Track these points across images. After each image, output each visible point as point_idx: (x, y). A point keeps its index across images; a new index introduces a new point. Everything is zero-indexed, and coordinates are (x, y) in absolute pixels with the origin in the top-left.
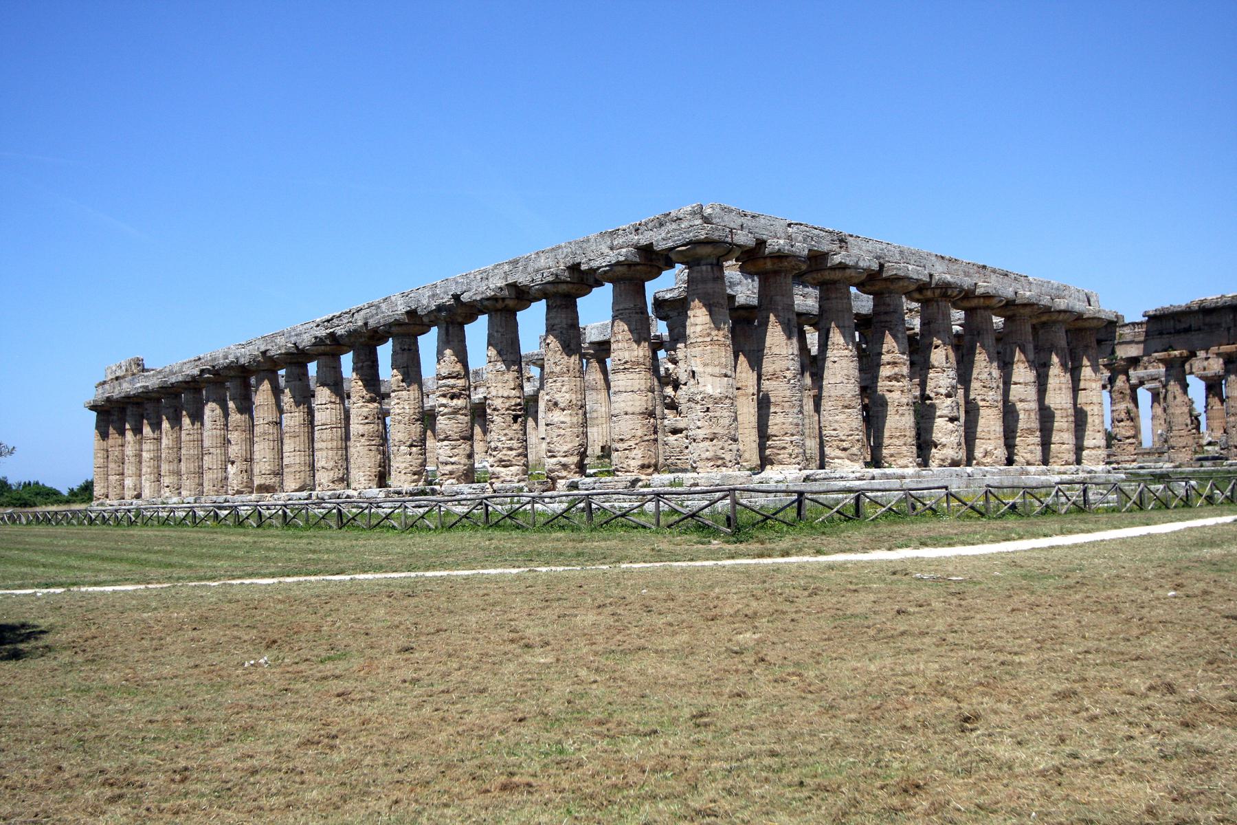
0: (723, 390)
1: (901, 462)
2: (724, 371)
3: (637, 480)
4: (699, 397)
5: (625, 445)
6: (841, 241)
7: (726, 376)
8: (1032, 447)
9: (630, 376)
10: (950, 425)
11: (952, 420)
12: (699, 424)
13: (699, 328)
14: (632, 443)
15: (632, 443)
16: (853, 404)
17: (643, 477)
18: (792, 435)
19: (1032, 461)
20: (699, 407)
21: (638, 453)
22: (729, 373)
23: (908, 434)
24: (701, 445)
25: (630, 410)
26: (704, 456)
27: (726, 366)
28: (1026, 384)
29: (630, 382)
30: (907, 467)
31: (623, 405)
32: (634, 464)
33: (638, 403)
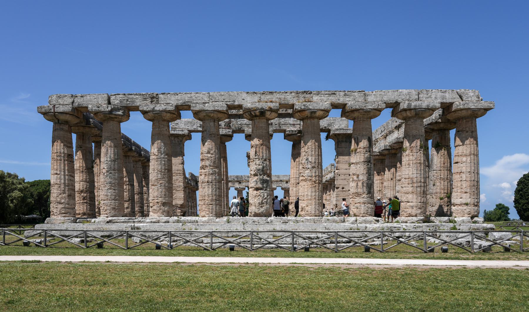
0: (55, 181)
1: (203, 213)
2: (55, 172)
6: (153, 97)
7: (56, 174)
8: (359, 205)
10: (255, 192)
11: (257, 189)
16: (156, 183)
18: (104, 200)
19: (357, 214)
22: (59, 172)
23: (206, 198)
27: (57, 170)
28: (357, 163)
30: (204, 216)
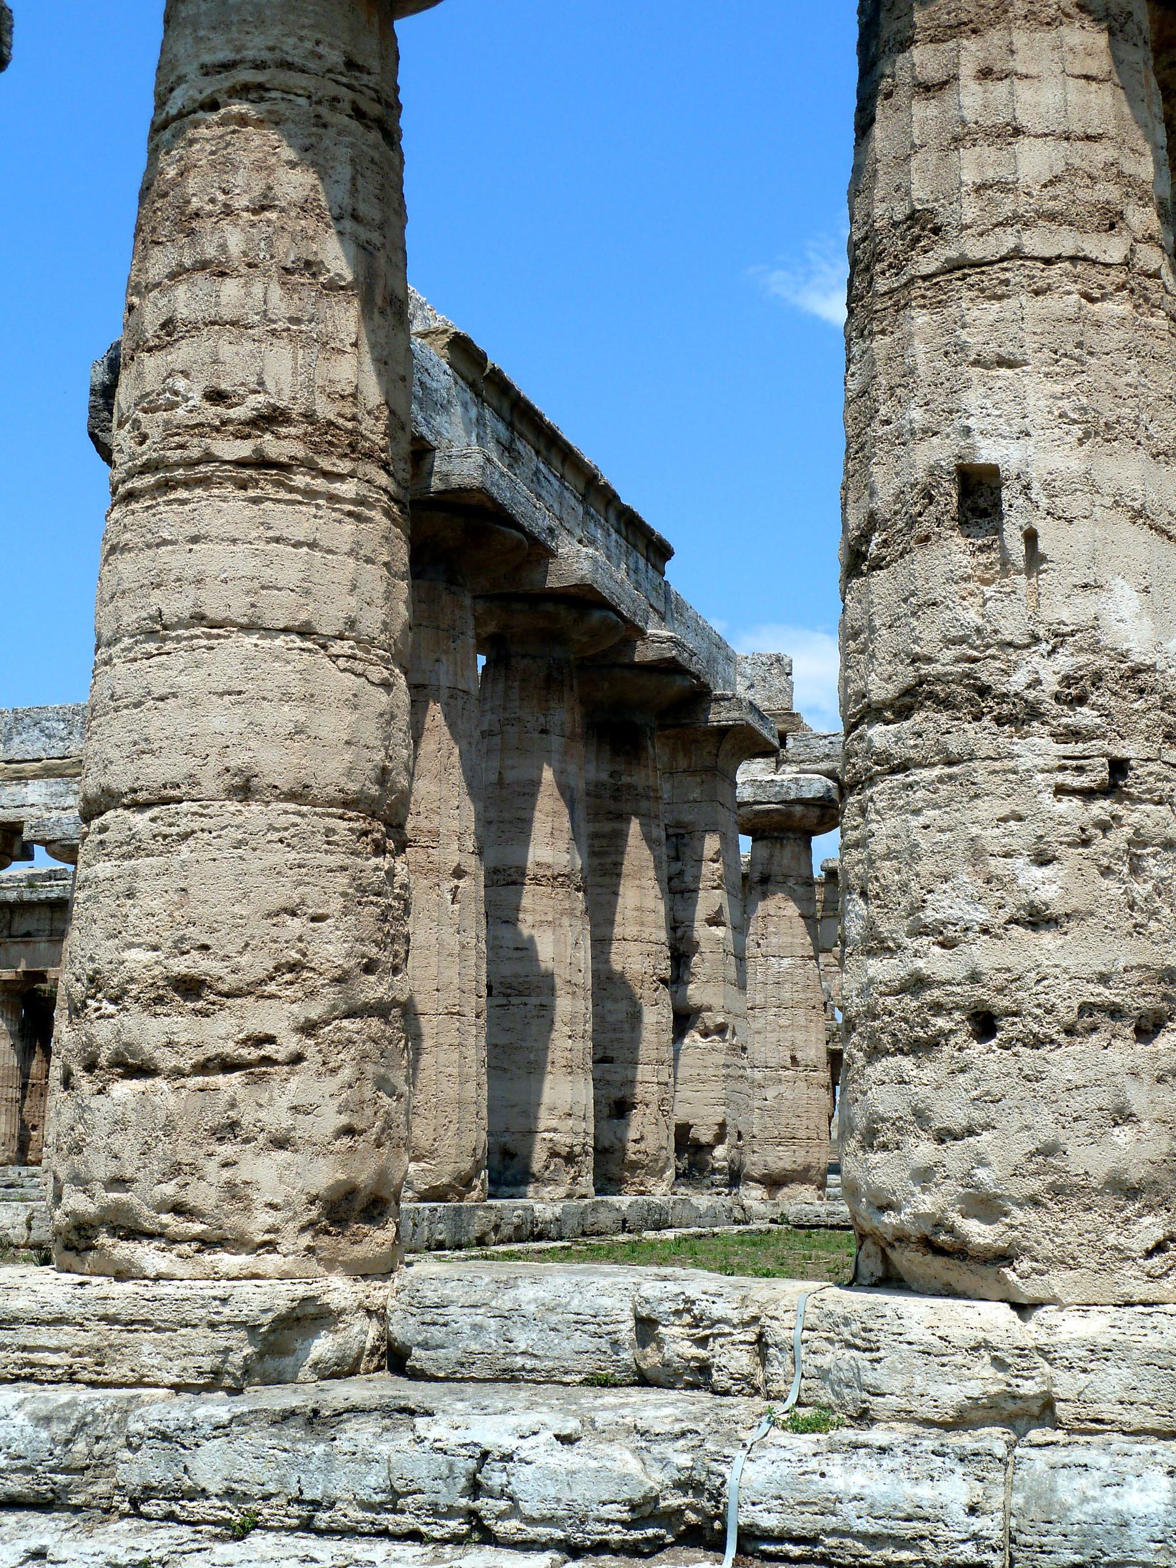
3: (309, 1317)
4: (1049, 670)
5: (221, 1032)
9: (298, 521)
12: (1045, 886)
13: (1034, 161)
14: (276, 1017)
15: (276, 1017)
17: (339, 1290)
20: (1037, 749)
21: (309, 1098)
24: (1066, 1062)
25: (275, 764)
26: (1089, 1159)
29: (290, 567)
31: (221, 719)
32: (282, 1182)
33: (333, 725)
